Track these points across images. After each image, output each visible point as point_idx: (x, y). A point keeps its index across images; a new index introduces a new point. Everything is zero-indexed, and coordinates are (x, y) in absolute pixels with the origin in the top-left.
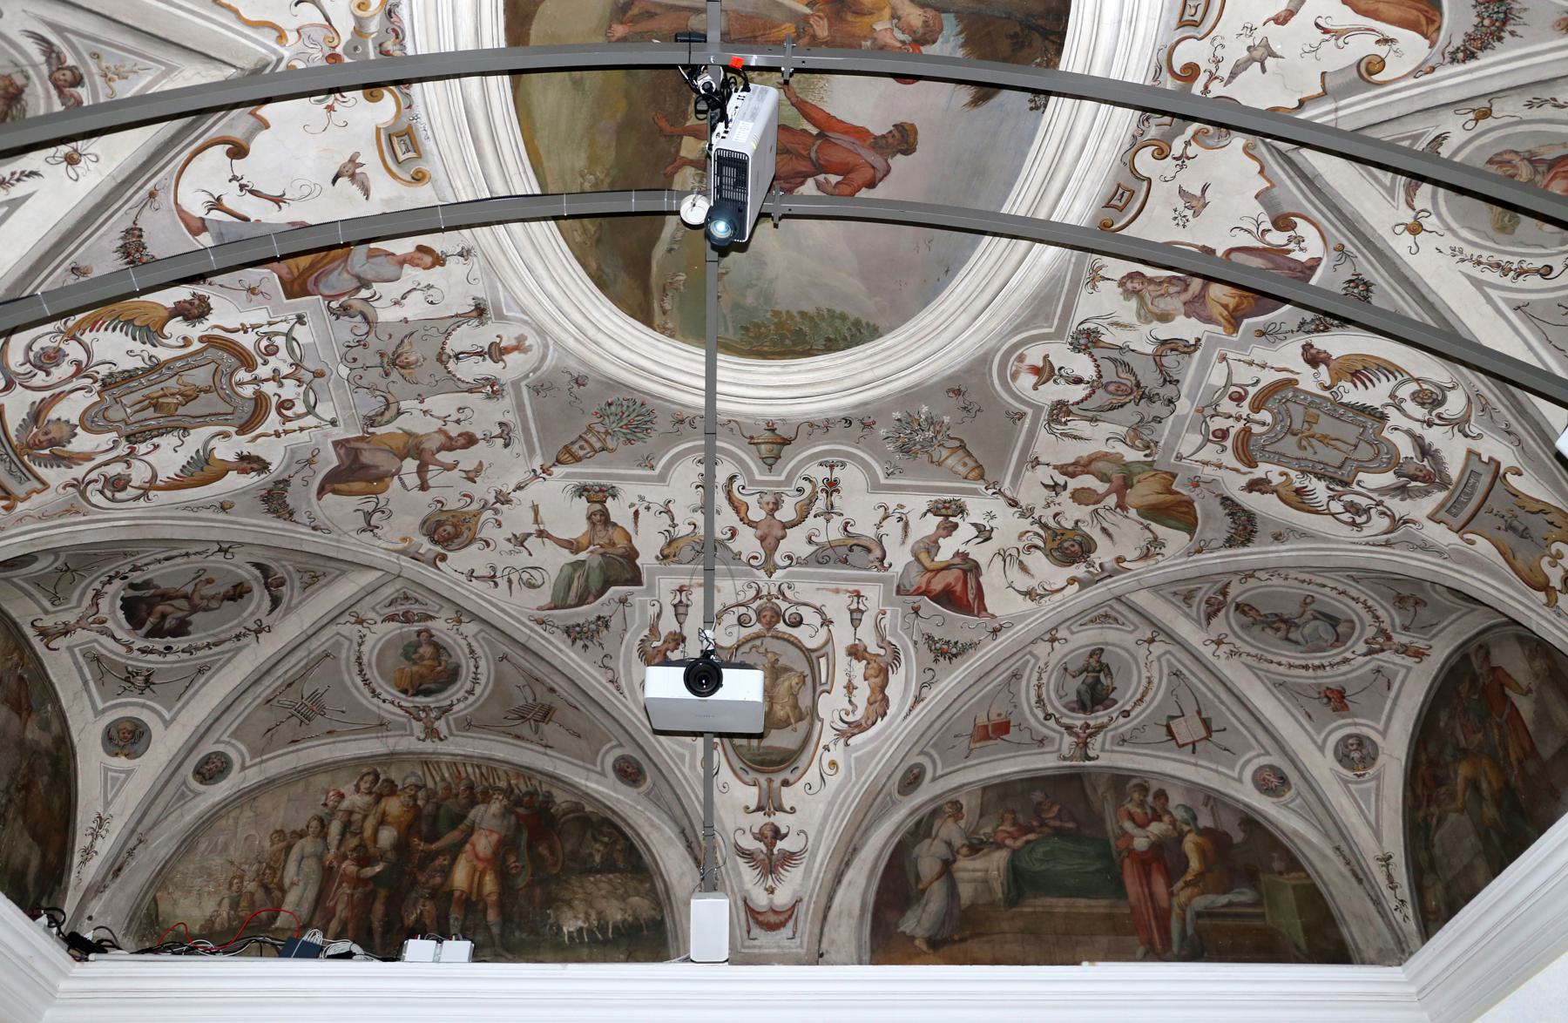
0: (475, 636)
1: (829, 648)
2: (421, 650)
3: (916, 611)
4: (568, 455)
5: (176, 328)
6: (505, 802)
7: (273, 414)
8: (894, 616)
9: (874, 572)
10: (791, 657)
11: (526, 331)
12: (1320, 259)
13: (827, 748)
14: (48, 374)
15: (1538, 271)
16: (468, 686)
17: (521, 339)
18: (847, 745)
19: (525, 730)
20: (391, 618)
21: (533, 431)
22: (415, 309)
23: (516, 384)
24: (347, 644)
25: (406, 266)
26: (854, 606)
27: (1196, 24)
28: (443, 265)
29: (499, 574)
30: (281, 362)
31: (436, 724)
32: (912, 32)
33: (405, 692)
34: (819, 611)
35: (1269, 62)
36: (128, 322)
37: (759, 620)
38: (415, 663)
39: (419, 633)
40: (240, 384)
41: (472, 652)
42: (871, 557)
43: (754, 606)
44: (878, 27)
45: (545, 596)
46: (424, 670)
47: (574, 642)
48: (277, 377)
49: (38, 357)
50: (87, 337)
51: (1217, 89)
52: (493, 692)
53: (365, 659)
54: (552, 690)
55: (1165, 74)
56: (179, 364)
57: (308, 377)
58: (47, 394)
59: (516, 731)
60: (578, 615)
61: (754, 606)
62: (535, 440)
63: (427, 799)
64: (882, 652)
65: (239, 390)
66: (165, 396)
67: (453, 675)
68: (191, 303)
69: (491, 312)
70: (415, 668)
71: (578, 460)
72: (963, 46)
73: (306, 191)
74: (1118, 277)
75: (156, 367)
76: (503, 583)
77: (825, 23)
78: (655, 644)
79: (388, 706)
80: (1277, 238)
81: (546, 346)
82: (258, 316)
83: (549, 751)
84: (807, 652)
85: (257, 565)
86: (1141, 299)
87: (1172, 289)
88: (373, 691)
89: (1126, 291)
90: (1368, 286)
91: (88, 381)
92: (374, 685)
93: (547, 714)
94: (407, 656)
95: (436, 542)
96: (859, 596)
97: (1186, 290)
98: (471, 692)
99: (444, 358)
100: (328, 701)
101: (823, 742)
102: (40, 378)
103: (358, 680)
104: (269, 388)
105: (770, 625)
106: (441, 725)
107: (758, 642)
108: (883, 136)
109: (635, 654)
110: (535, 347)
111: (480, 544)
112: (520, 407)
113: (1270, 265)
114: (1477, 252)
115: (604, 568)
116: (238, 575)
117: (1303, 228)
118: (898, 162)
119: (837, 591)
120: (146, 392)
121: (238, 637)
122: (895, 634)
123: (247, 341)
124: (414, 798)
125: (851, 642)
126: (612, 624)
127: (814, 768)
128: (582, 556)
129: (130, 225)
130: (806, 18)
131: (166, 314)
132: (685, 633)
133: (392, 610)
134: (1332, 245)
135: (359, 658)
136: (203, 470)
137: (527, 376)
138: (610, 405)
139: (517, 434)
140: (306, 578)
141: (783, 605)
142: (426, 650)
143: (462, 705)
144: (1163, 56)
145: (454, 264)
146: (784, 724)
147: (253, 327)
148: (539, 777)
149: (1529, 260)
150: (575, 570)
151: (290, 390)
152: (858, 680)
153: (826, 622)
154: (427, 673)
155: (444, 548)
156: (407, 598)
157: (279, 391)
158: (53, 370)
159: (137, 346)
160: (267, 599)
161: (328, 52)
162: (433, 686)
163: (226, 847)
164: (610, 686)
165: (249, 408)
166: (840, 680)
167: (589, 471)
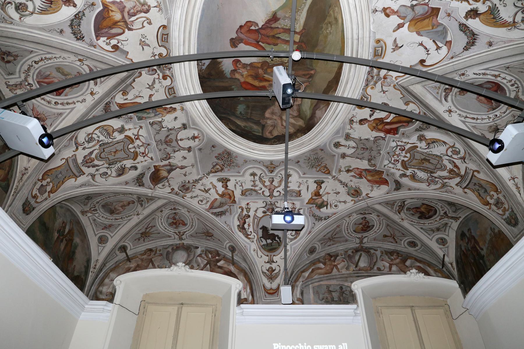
12: (97, 40)
15: (38, 62)
25: (396, 11)
27: (169, 89)
28: (384, 8)
32: (237, 72)
35: (148, 86)
44: (246, 73)
51: (156, 76)
55: (170, 75)
72: (223, 71)
73: (411, 45)
74: (152, 9)
77: (260, 73)
80: (114, 42)
86: (140, 3)
87: (132, 11)
89: (147, 4)
90: (78, 39)
97: (128, 12)
108: (240, 43)
113: (109, 32)
114: (58, 60)
117: (109, 48)
118: (234, 36)
129: (465, 52)
130: (265, 74)
134: (97, 46)
144: (173, 80)
145: (380, 7)
149: (43, 64)
161: (386, 80)
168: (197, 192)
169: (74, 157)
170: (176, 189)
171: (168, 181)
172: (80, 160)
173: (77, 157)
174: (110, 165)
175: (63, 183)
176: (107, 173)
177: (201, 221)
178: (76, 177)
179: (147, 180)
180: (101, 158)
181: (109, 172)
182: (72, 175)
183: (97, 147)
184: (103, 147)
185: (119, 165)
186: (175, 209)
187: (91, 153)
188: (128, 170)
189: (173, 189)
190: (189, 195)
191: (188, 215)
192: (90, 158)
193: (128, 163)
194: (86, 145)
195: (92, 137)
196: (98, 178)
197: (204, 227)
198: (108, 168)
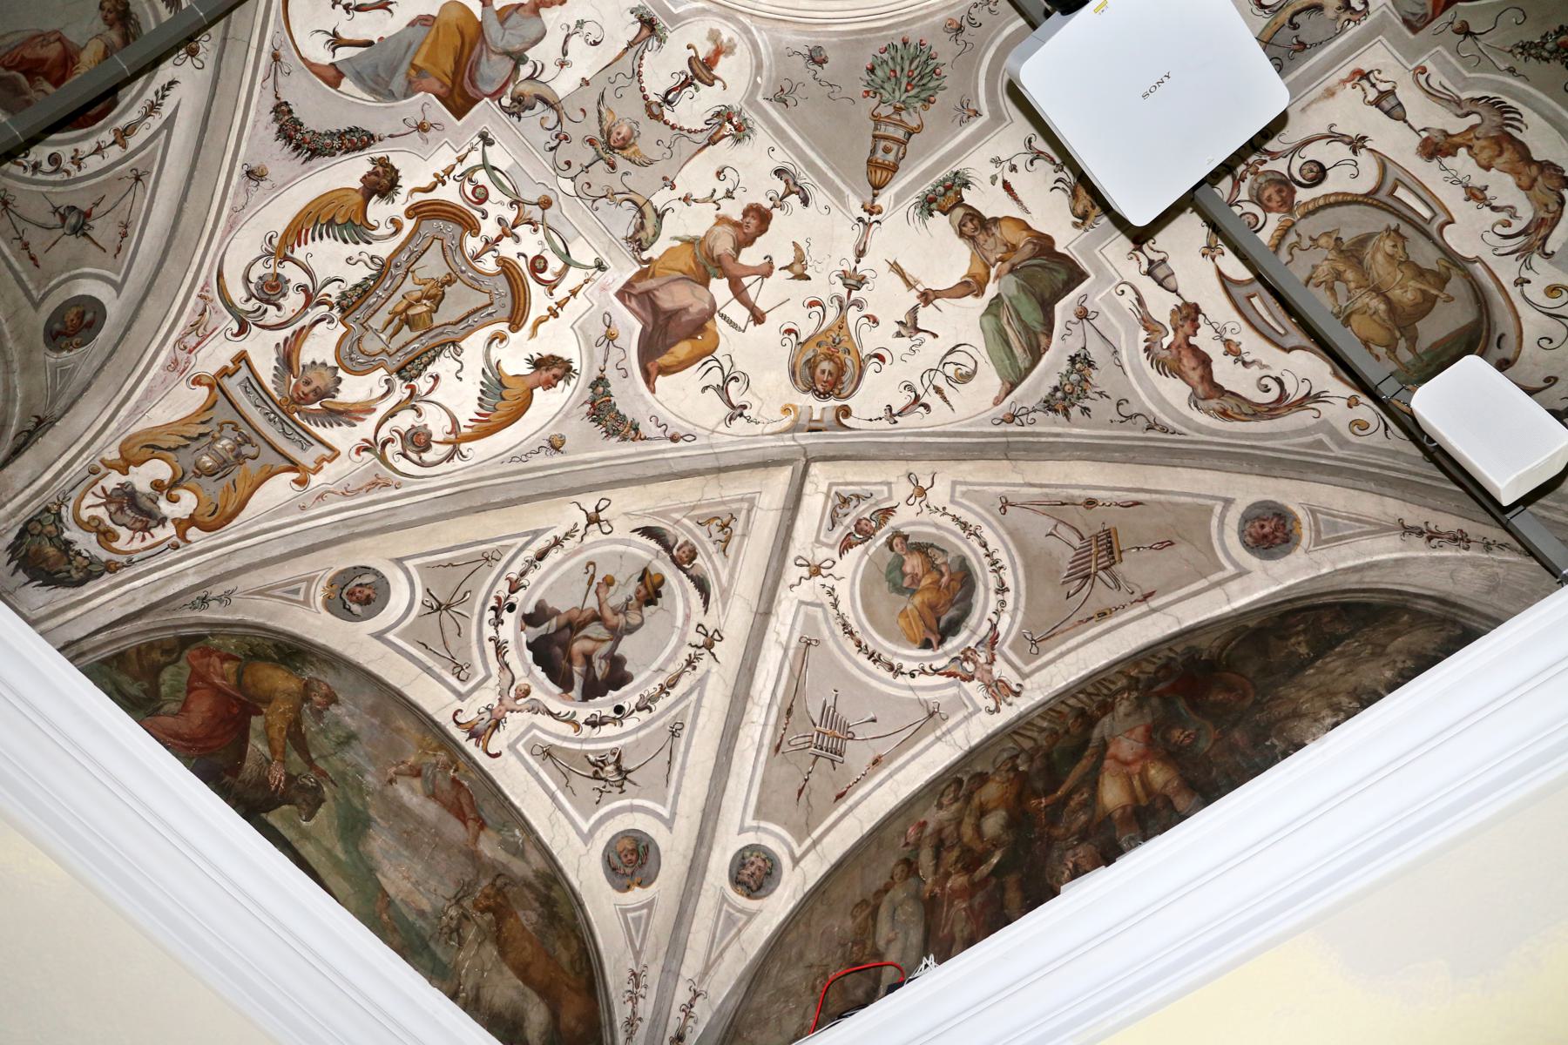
0: (953, 501)
1: (1393, 172)
2: (908, 569)
3: (1465, 31)
4: (880, 173)
5: (378, 211)
6: (1135, 694)
7: (534, 286)
8: (1443, 65)
9: (1353, 30)
10: (1353, 223)
11: (715, 23)
13: (1521, 282)
14: (279, 308)
16: (993, 585)
17: (714, 36)
18: (1548, 256)
19: (1103, 594)
20: (846, 546)
21: (820, 163)
22: (585, 62)
23: (751, 101)
24: (819, 613)
26: (1372, 95)
29: (920, 391)
30: (498, 207)
31: (996, 674)
33: (927, 644)
34: (1332, 137)
36: (331, 222)
37: (1267, 209)
38: (913, 592)
39: (890, 544)
40: (477, 257)
41: (965, 526)
42: (1330, 13)
43: (1244, 194)
45: (990, 380)
46: (928, 596)
47: (1067, 414)
48: (508, 231)
49: (260, 289)
50: (299, 253)
52: (1027, 567)
53: (852, 621)
54: (1091, 503)
56: (403, 257)
57: (536, 213)
58: (288, 332)
59: (1091, 608)
60: (1046, 373)
61: (1244, 194)
62: (830, 174)
63: (1031, 759)
64: (1474, 119)
65: (478, 265)
66: (410, 305)
67: (965, 579)
68: (374, 173)
69: (661, 21)
70: (917, 600)
71: (893, 169)
75: (384, 269)
76: (931, 398)
78: (1166, 342)
79: (922, 680)
81: (746, 30)
82: (443, 158)
83: (1154, 603)
84: (1368, 199)
85: (648, 532)
88: (891, 668)
91: (325, 308)
92: (886, 656)
93: (1107, 547)
94: (898, 589)
95: (824, 395)
96: (1365, 76)
98: (1002, 589)
99: (655, 110)
100: (847, 712)
101: (1507, 280)
102: (272, 316)
103: (862, 659)
104: (507, 248)
105: (1287, 204)
106: (1001, 670)
107: (1292, 238)
109: (1152, 373)
110: (736, 39)
111: (872, 366)
112: (779, 133)
115: (1029, 285)
116: (634, 557)
119: (1330, 93)
120: (390, 306)
121: (690, 663)
122: (1468, 84)
123: (449, 193)
124: (1015, 768)
125: (1417, 141)
126: (1093, 356)
127: (1529, 316)
128: (992, 290)
131: (359, 198)
132: (1190, 299)
133: (839, 532)
135: (845, 625)
136: (503, 402)
137: (755, 84)
138: (872, 70)
139: (806, 179)
140: (714, 528)
141: (1280, 166)
142: (913, 563)
143: (1005, 620)
146: (1426, 305)
147: (448, 172)
148: (1166, 646)
150: (997, 316)
151: (531, 243)
152: (1478, 177)
153: (1357, 144)
154: (933, 593)
155: (838, 397)
156: (846, 501)
157: (521, 248)
158: (282, 301)
159: (351, 249)
160: (690, 585)
162: (953, 612)
163: (801, 956)
164: (1151, 434)
165: (502, 286)
166: (1452, 198)
167: (915, 176)
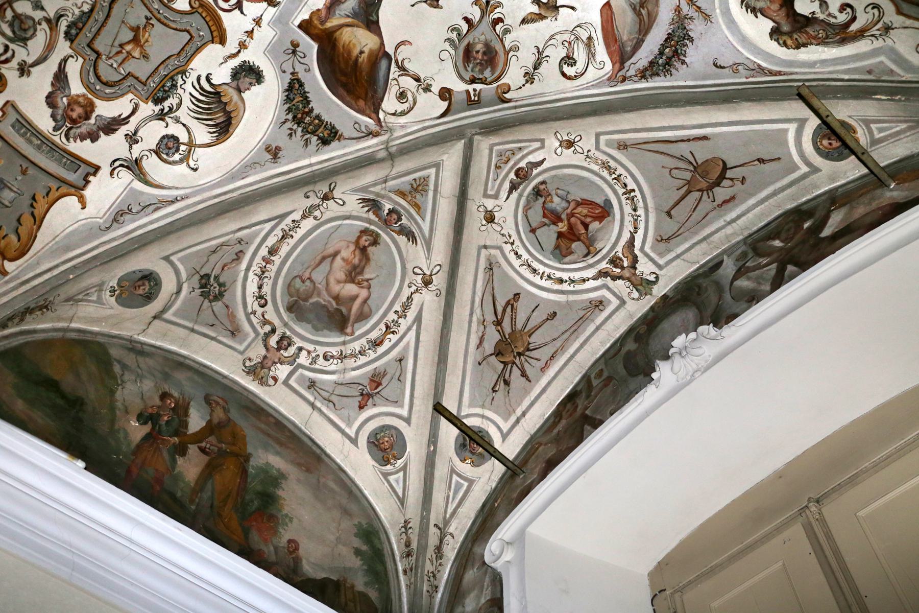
168: (526, 39)
169: (9, 109)
170: (459, 87)
171: (402, 68)
172: (43, 121)
173: (23, 107)
174: (157, 101)
175: (38, 222)
176: (175, 139)
177: (637, 145)
178: (78, 189)
179: (326, 102)
180: (107, 84)
181: (175, 129)
182: (54, 185)
183: (63, 48)
184: (83, 40)
185: (187, 89)
186: (522, 175)
187: (60, 78)
188: (232, 93)
189: (445, 94)
190: (513, 76)
191: (579, 160)
192: (73, 102)
193: (212, 65)
194: (21, 54)
195: (17, 16)
196: (152, 165)
197: (671, 163)
198: (161, 116)
